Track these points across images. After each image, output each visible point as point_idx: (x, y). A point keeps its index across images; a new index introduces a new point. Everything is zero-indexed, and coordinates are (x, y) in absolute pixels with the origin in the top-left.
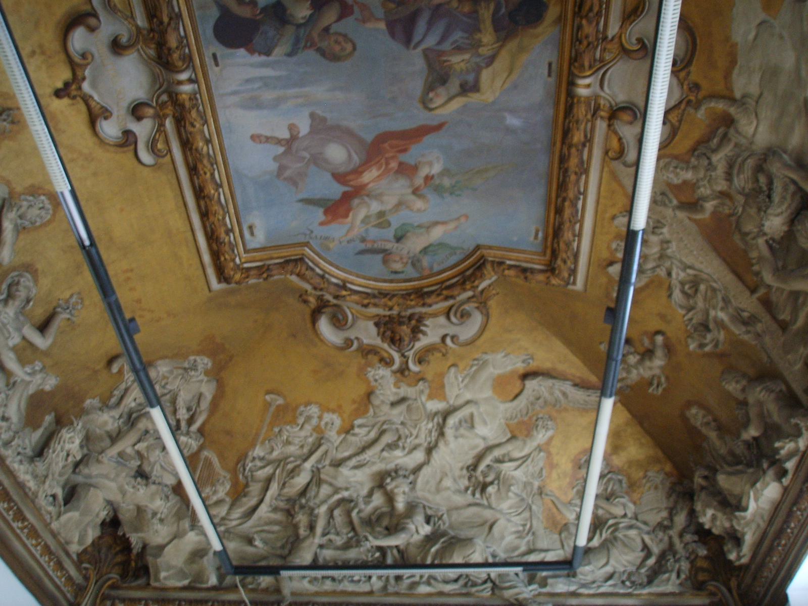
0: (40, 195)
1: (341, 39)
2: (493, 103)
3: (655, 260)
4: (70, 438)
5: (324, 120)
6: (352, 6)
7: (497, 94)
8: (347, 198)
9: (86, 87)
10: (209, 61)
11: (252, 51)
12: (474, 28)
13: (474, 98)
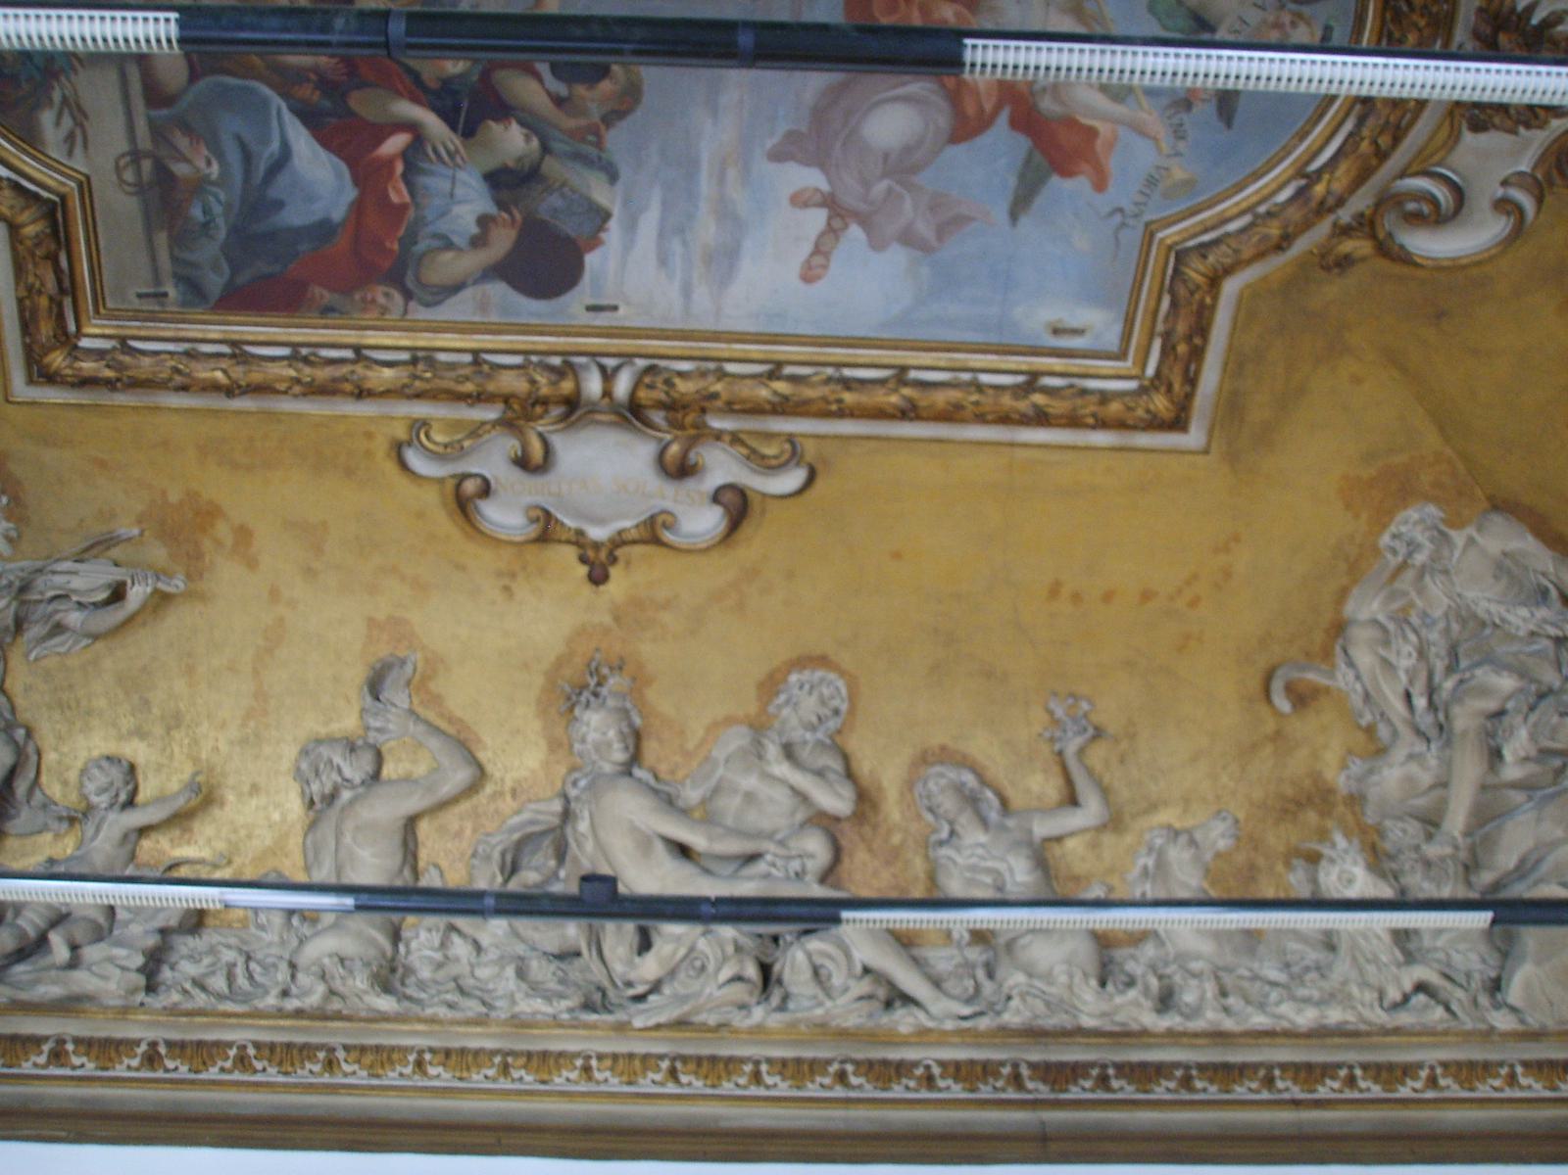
0: (785, 681)
4: (1340, 878)
5: (792, 136)
9: (597, 533)
10: (602, 320)
11: (594, 242)
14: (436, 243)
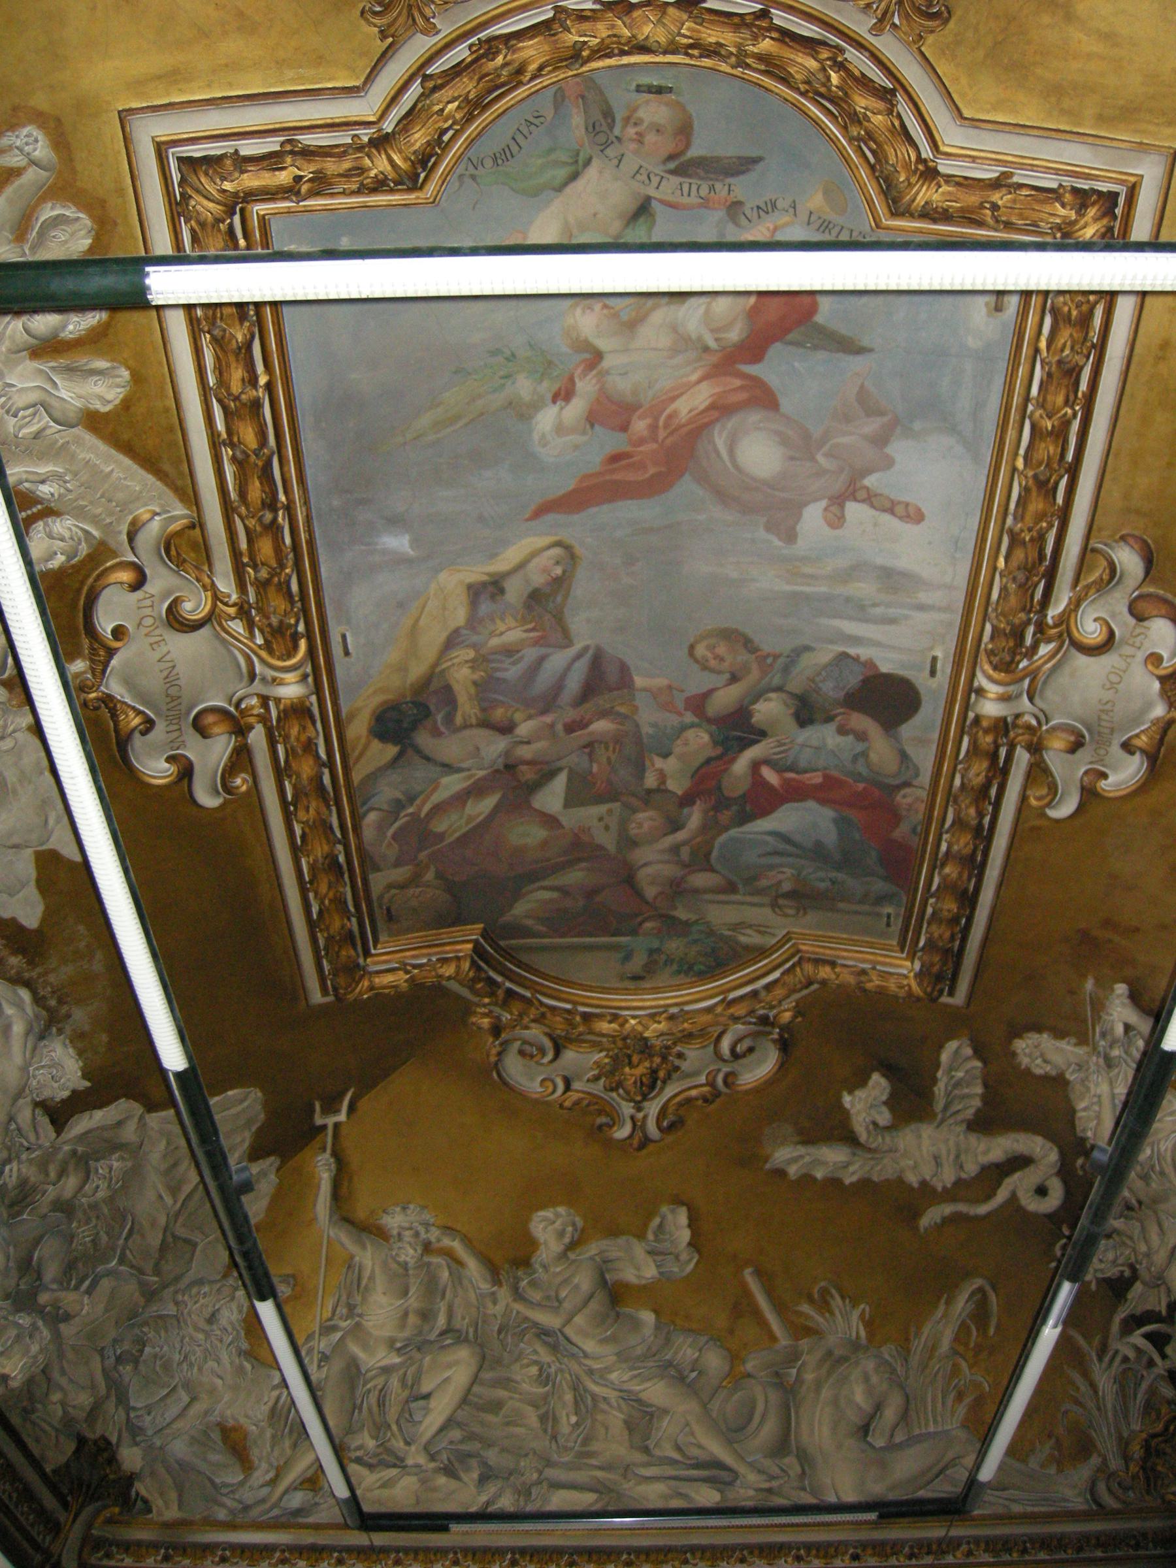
1: (713, 663)
2: (437, 571)
6: (686, 709)
7: (433, 587)
8: (754, 348)
11: (870, 664)
12: (485, 688)
13: (476, 572)
14: (861, 760)
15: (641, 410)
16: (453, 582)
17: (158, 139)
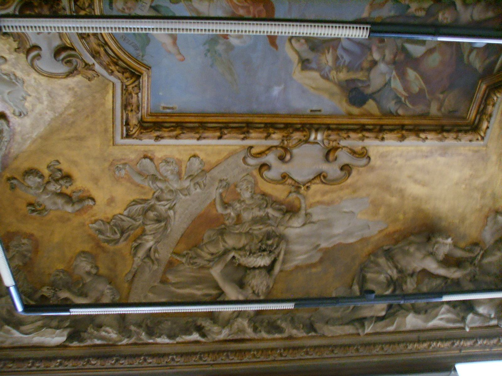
3: (167, 187)
13: (296, 67)
15: (235, 11)
16: (298, 75)
17: (125, 135)
